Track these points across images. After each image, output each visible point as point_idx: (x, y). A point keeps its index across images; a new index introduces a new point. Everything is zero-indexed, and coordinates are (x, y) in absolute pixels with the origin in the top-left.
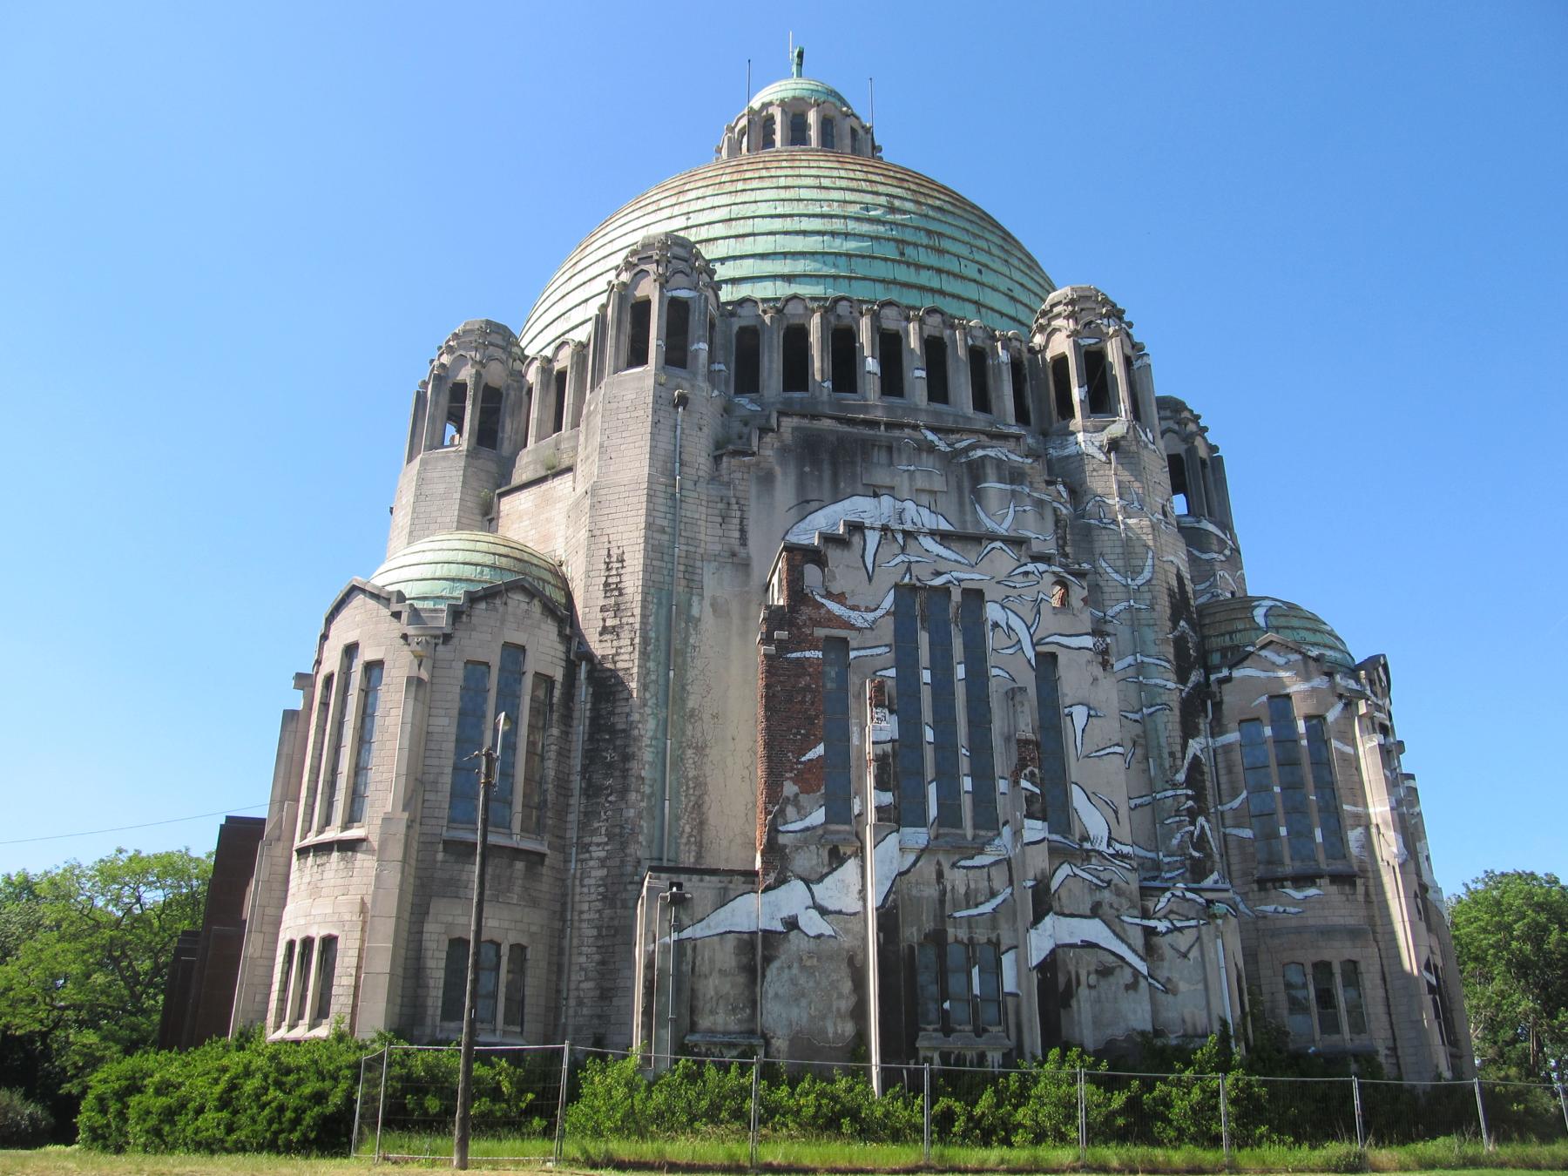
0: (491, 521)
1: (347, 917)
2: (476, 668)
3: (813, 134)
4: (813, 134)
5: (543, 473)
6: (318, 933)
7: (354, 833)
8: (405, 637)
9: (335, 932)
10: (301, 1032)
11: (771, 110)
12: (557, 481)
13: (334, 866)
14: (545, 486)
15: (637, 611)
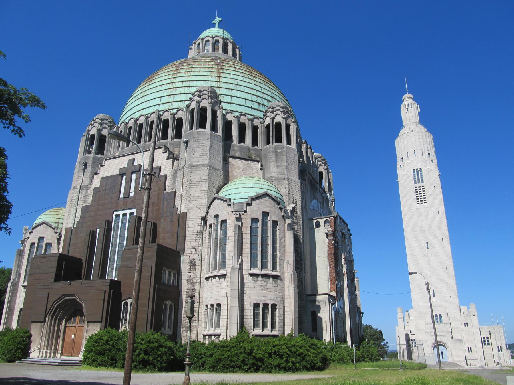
0: (226, 164)
1: (279, 299)
2: (254, 220)
3: (238, 57)
4: (238, 57)
5: (247, 158)
6: (270, 302)
7: (274, 273)
8: (283, 216)
9: (276, 303)
10: (267, 331)
11: (228, 41)
12: (252, 163)
13: (271, 282)
14: (247, 162)
15: (301, 220)
